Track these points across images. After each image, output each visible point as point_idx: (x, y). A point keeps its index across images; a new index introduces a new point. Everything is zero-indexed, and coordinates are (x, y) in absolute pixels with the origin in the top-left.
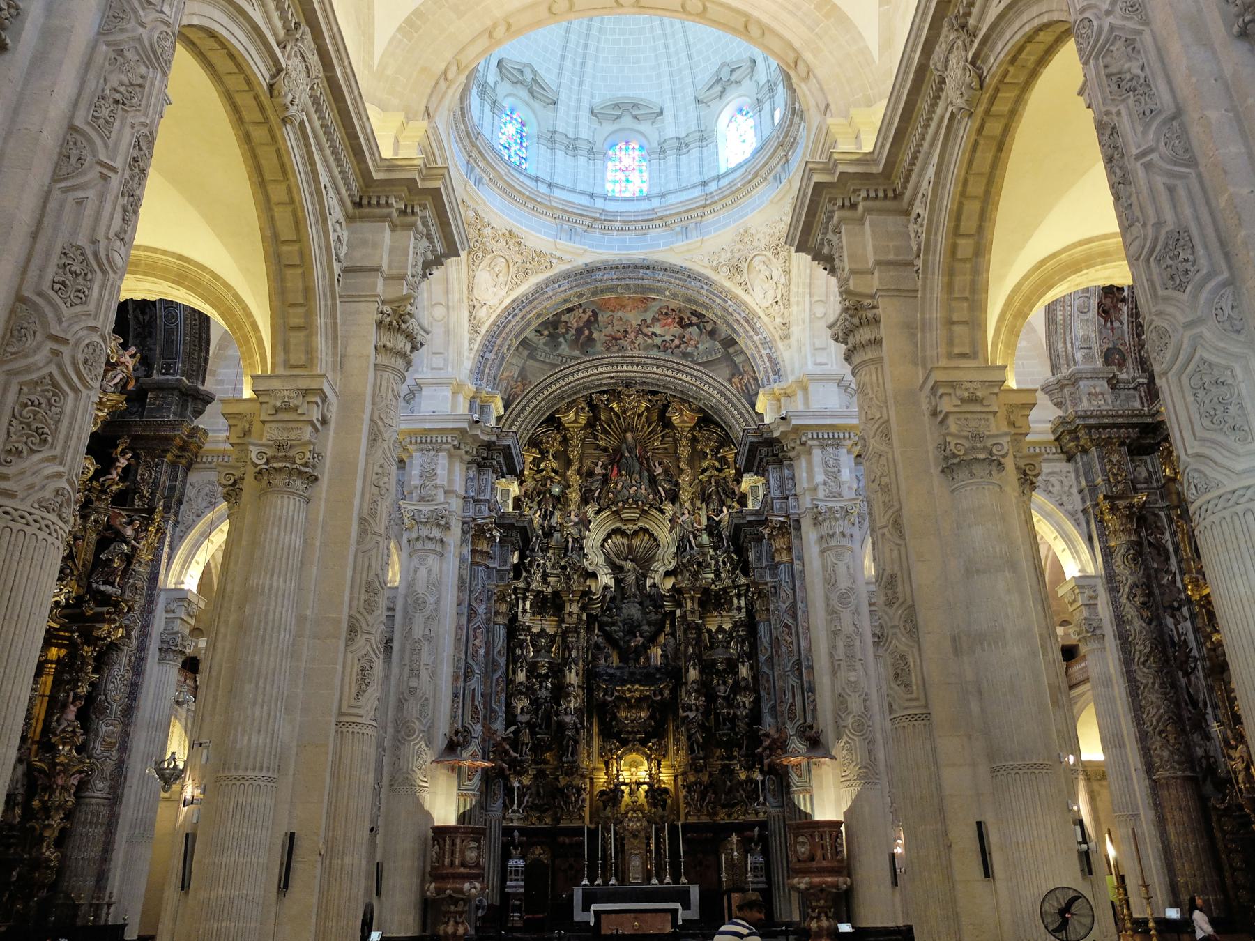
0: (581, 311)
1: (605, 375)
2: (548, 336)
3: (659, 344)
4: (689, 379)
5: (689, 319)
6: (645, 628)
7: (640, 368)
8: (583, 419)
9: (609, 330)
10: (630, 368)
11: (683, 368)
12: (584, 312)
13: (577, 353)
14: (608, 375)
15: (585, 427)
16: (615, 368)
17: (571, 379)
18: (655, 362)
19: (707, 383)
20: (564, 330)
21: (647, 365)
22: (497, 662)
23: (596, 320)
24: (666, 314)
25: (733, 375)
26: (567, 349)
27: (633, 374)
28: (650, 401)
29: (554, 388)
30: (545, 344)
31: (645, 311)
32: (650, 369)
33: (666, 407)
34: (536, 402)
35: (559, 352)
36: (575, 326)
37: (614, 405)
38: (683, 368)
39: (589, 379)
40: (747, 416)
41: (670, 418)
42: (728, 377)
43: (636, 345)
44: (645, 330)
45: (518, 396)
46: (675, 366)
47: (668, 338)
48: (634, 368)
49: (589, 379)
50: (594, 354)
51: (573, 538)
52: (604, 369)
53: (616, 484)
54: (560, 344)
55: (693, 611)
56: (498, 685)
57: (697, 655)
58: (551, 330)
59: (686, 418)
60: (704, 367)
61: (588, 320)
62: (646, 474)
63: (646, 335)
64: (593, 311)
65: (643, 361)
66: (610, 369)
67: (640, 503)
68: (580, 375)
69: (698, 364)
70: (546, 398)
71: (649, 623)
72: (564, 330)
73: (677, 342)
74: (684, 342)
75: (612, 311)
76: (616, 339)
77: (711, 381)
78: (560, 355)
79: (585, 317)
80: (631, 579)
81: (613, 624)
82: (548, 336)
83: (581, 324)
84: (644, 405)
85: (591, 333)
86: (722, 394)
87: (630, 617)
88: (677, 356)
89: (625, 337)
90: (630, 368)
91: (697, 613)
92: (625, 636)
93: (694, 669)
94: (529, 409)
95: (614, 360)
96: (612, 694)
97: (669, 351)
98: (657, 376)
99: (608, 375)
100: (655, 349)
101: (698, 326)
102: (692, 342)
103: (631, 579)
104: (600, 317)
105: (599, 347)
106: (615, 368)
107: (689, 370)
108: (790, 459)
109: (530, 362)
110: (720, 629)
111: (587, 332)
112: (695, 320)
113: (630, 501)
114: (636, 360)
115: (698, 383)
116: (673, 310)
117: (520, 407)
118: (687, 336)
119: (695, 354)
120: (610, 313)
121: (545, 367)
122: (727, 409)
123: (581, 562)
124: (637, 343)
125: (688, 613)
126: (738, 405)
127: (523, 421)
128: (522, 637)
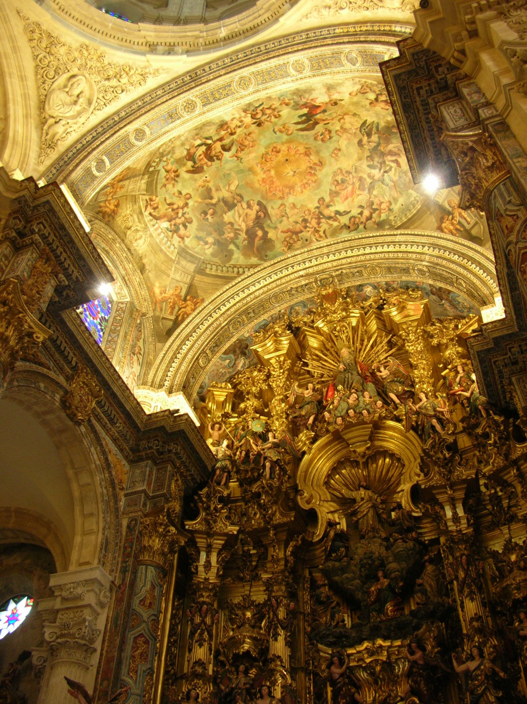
0: (245, 205)
1: (292, 277)
2: (214, 244)
3: (347, 223)
4: (391, 249)
5: (369, 176)
6: (393, 565)
7: (332, 257)
8: (285, 343)
9: (286, 224)
10: (320, 261)
11: (381, 240)
12: (249, 206)
13: (254, 260)
14: (296, 275)
15: (288, 355)
16: (302, 266)
17: (252, 289)
18: (347, 244)
19: (413, 243)
20: (232, 235)
21: (339, 251)
22: (136, 614)
23: (266, 214)
24: (343, 181)
25: (442, 220)
26: (242, 258)
27: (325, 266)
28: (363, 308)
29: (232, 302)
30: (213, 255)
31: (318, 184)
32: (343, 254)
33: (381, 308)
34: (211, 320)
35: (232, 262)
36: (244, 226)
37: (320, 324)
38: (381, 240)
39: (274, 285)
40: (471, 253)
41: (388, 314)
42: (436, 225)
43: (321, 233)
44: (327, 212)
45: (188, 315)
46: (372, 241)
47: (355, 212)
48: (326, 259)
49: (274, 285)
50: (275, 257)
51: (271, 462)
52: (291, 270)
53: (333, 403)
54: (231, 253)
55: (456, 519)
56: (135, 648)
57: (473, 580)
58: (215, 235)
59: (412, 313)
60: (407, 228)
61: (258, 217)
62: (371, 386)
63: (330, 218)
64: (259, 204)
65: (333, 248)
66: (297, 268)
67: (365, 412)
68: (264, 282)
69: (399, 228)
70: (224, 313)
71: (397, 558)
72: (232, 235)
73: (366, 213)
74: (375, 210)
75: (282, 198)
76: (297, 233)
77: (417, 239)
78: (235, 266)
79: (252, 214)
80: (364, 508)
81: (343, 570)
82: (214, 244)
83: (251, 223)
84: (356, 313)
85: (266, 233)
86: (435, 246)
87: (369, 556)
88: (371, 230)
89: (306, 227)
90: (320, 261)
91: (464, 521)
92: (364, 583)
93: (472, 600)
94: (203, 328)
95: (299, 258)
96: (341, 663)
97: (361, 227)
98: (354, 259)
99: (296, 275)
100: (345, 231)
101: (383, 182)
102: (384, 206)
103: (364, 508)
104: (270, 210)
105: (279, 247)
106: (301, 267)
107: (389, 239)
108: (466, 77)
109: (198, 277)
110: (509, 547)
111: (260, 233)
112: (376, 173)
113: (351, 412)
114: (325, 250)
115: (403, 248)
116: (349, 173)
117: (191, 327)
118: (376, 201)
119: (392, 218)
120: (280, 202)
121: (219, 281)
122: (445, 259)
123: (295, 497)
124: (322, 230)
125: (450, 523)
126: (457, 247)
127: (197, 340)
128: (202, 599)
